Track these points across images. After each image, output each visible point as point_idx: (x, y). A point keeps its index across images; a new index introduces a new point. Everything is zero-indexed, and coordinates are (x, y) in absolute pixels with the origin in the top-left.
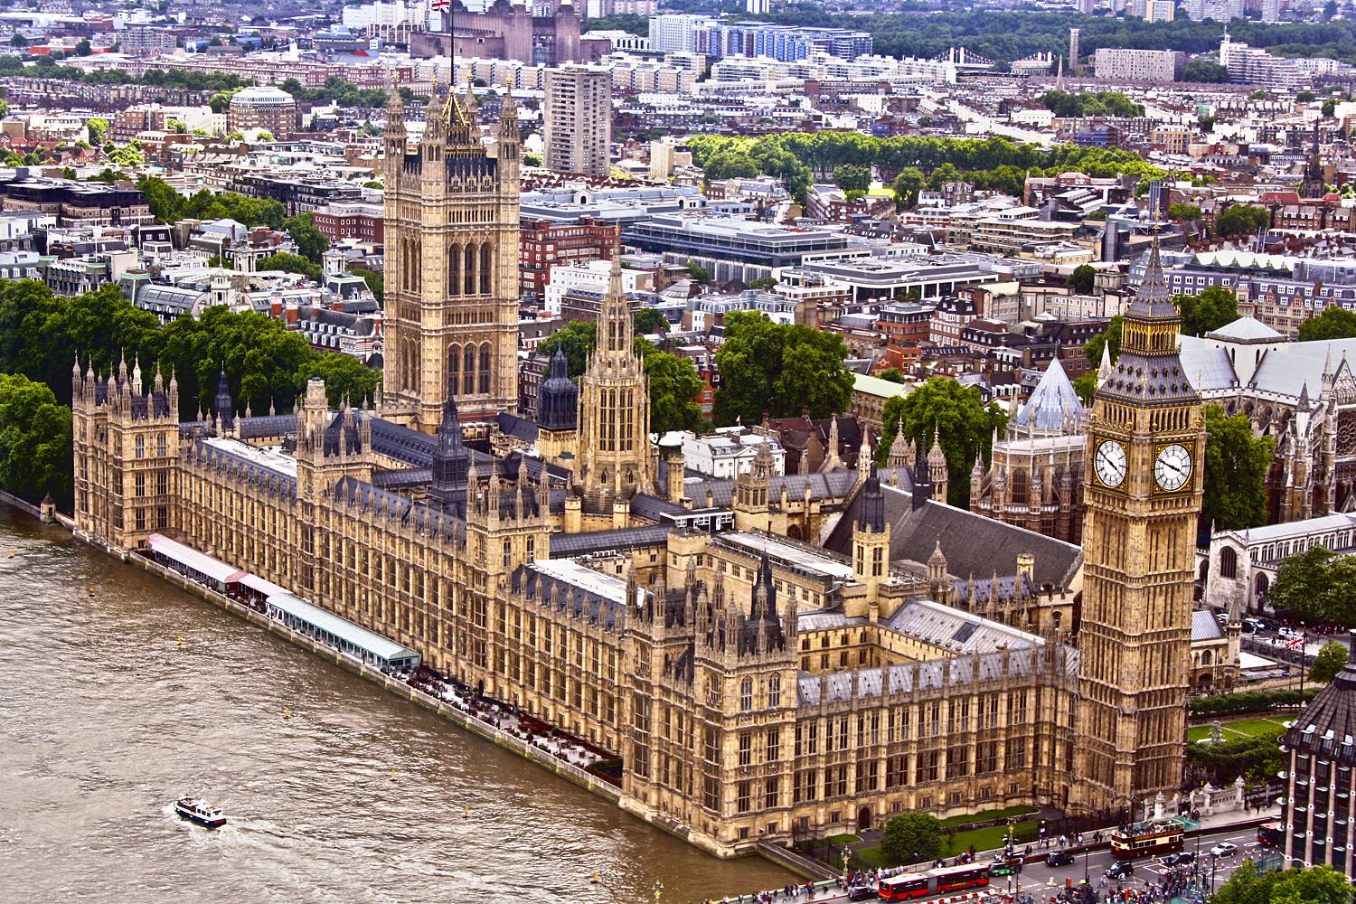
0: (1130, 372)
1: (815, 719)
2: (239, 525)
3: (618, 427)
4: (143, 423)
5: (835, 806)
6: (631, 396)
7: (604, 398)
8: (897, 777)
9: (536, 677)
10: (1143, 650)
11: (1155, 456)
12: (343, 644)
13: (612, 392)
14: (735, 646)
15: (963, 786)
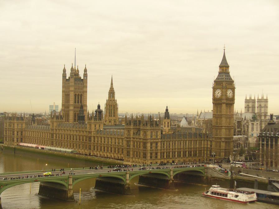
0: (221, 76)
1: (164, 141)
2: (38, 138)
3: (113, 112)
4: (18, 122)
5: (168, 160)
6: (115, 107)
7: (110, 106)
8: (179, 156)
9: (102, 149)
10: (226, 129)
11: (227, 91)
12: (61, 151)
13: (112, 106)
14: (149, 124)
15: (190, 158)
